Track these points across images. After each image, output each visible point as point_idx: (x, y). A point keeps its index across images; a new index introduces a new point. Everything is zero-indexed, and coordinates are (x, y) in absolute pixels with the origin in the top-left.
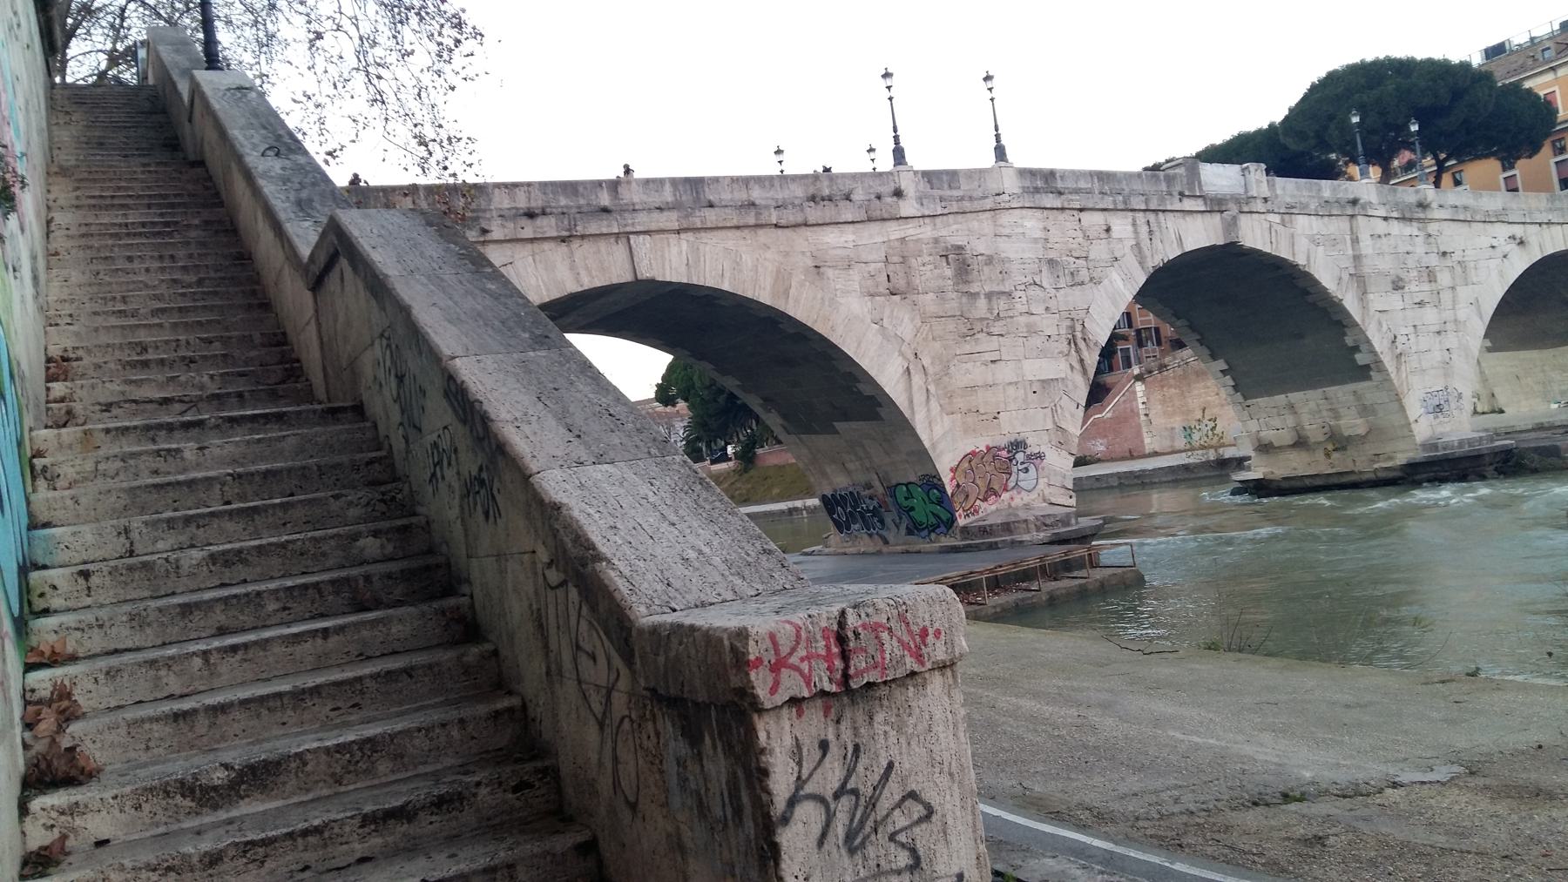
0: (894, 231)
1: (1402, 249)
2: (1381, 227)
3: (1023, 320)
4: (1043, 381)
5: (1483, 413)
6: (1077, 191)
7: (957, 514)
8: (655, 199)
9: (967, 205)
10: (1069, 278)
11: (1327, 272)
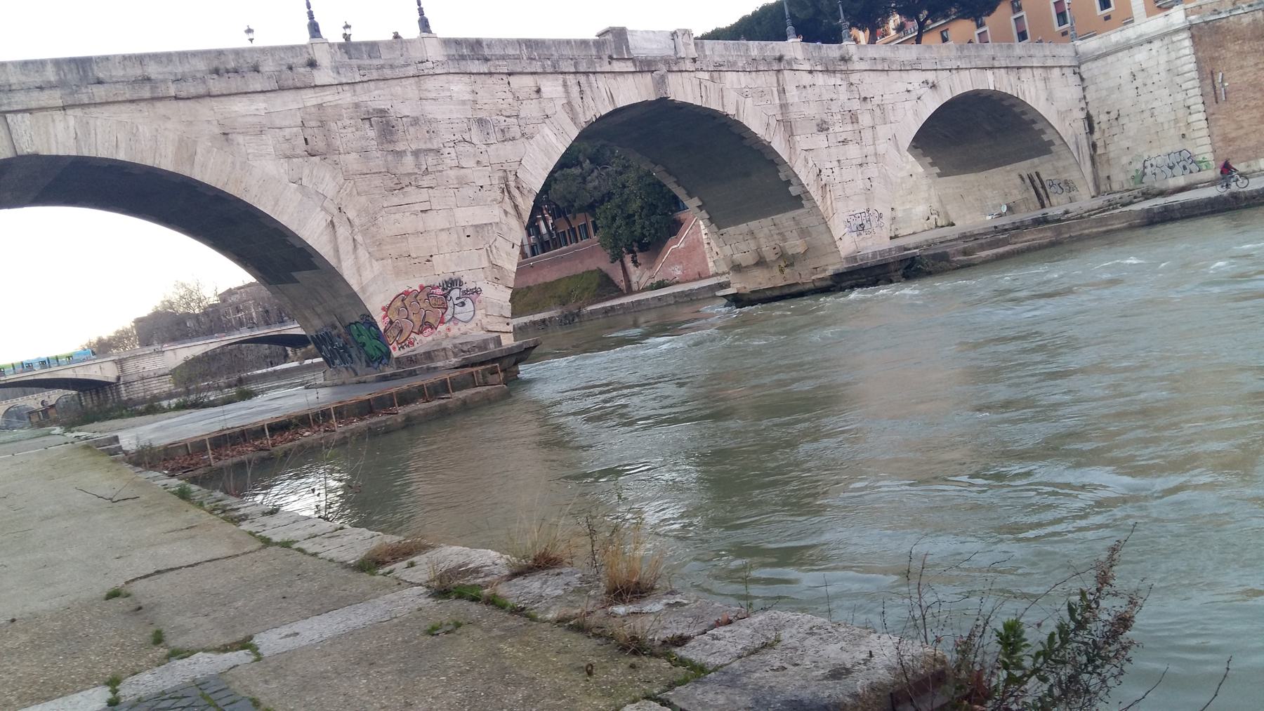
0: (310, 99)
1: (826, 96)
2: (806, 79)
3: (452, 173)
4: (476, 226)
5: (942, 227)
6: (503, 58)
7: (391, 347)
8: (36, 79)
9: (388, 73)
10: (499, 136)
11: (756, 119)
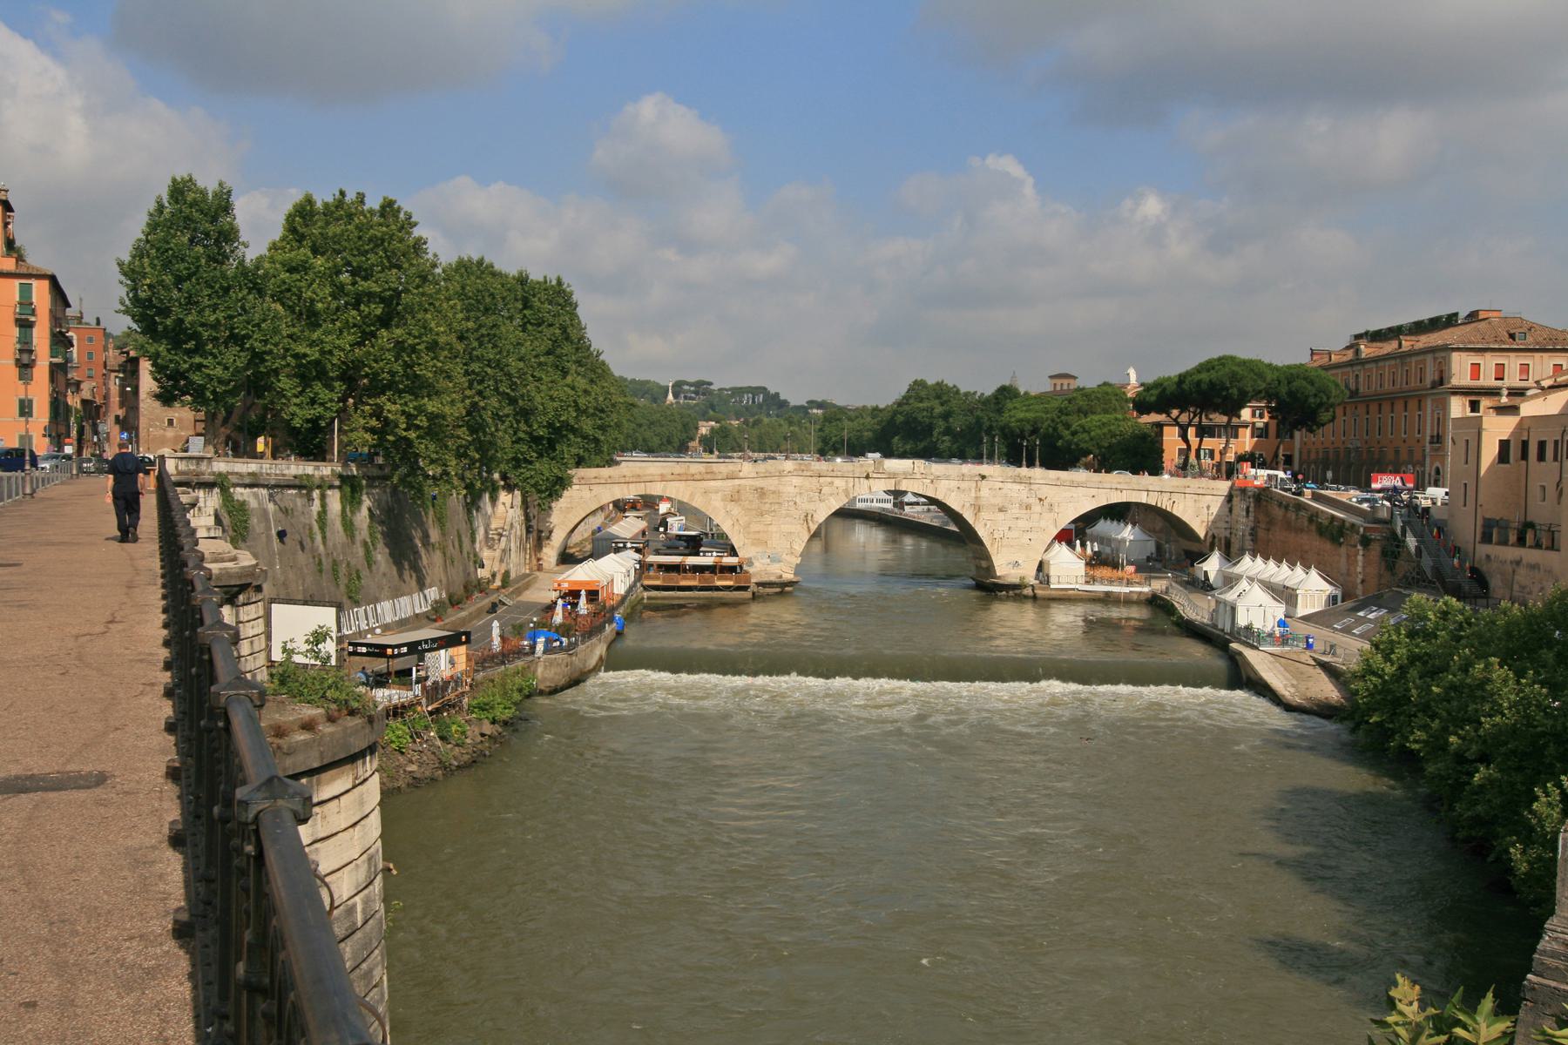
0: (737, 482)
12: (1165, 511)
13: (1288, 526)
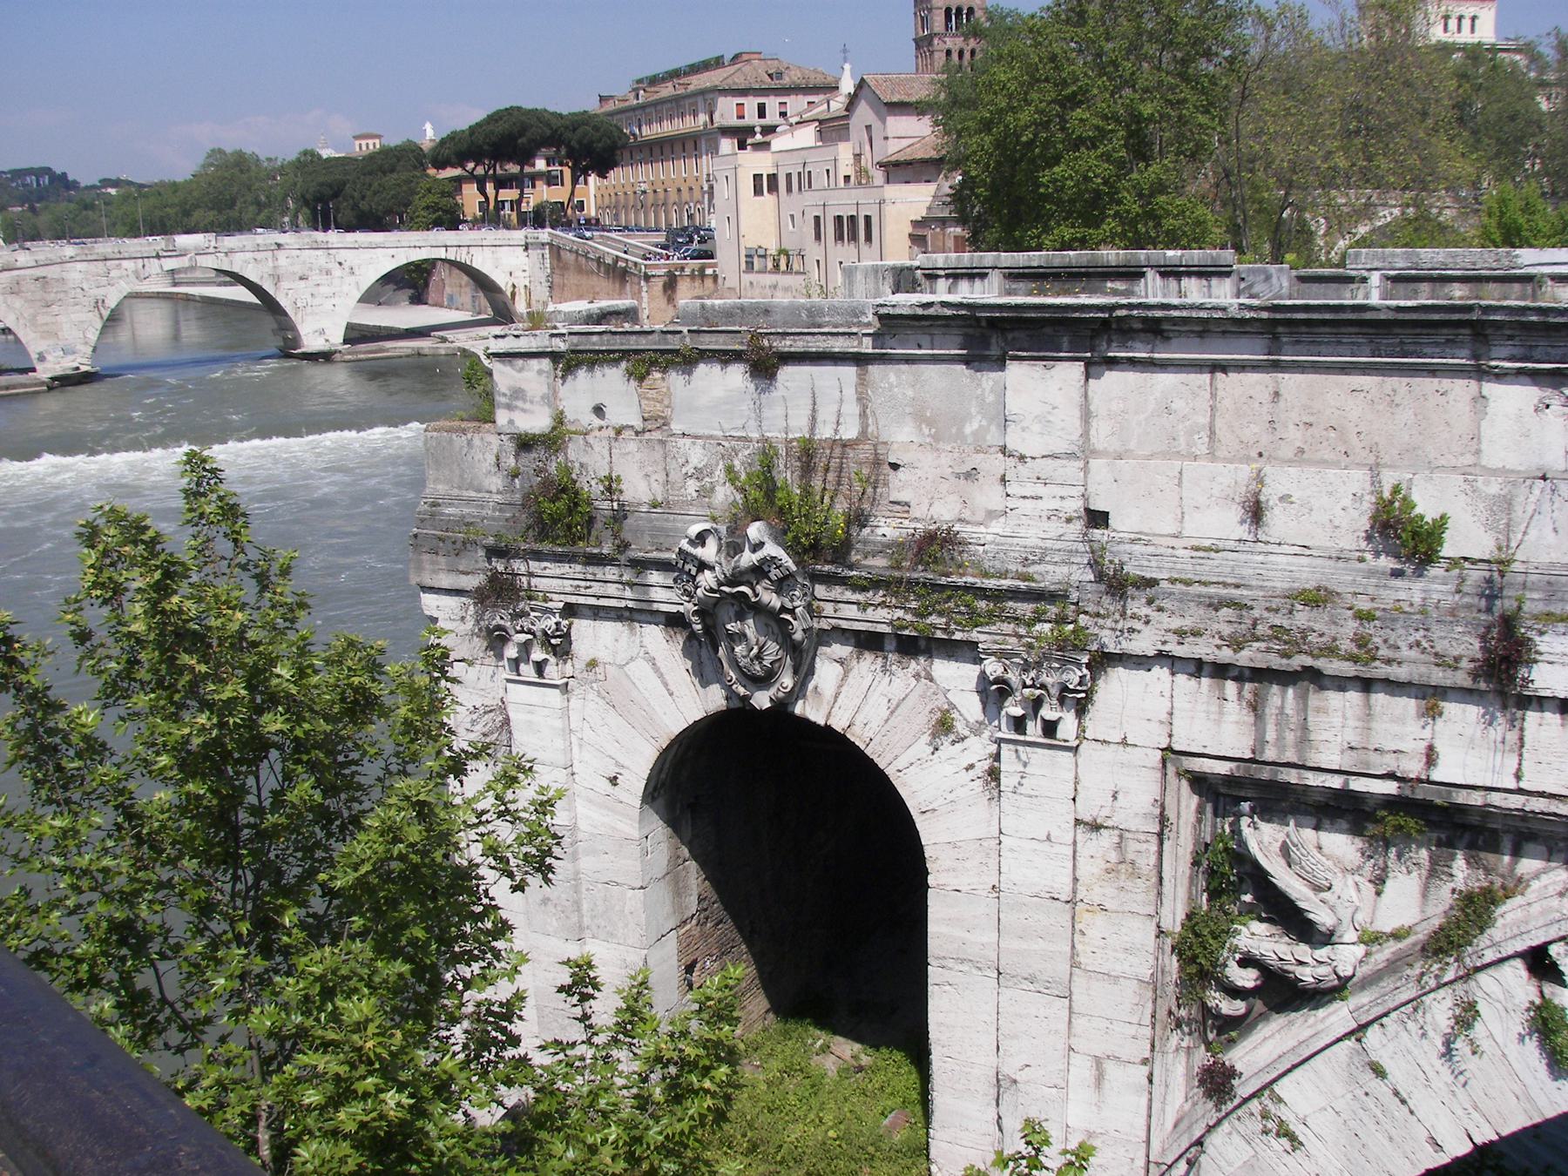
12: (465, 264)
13: (580, 270)
